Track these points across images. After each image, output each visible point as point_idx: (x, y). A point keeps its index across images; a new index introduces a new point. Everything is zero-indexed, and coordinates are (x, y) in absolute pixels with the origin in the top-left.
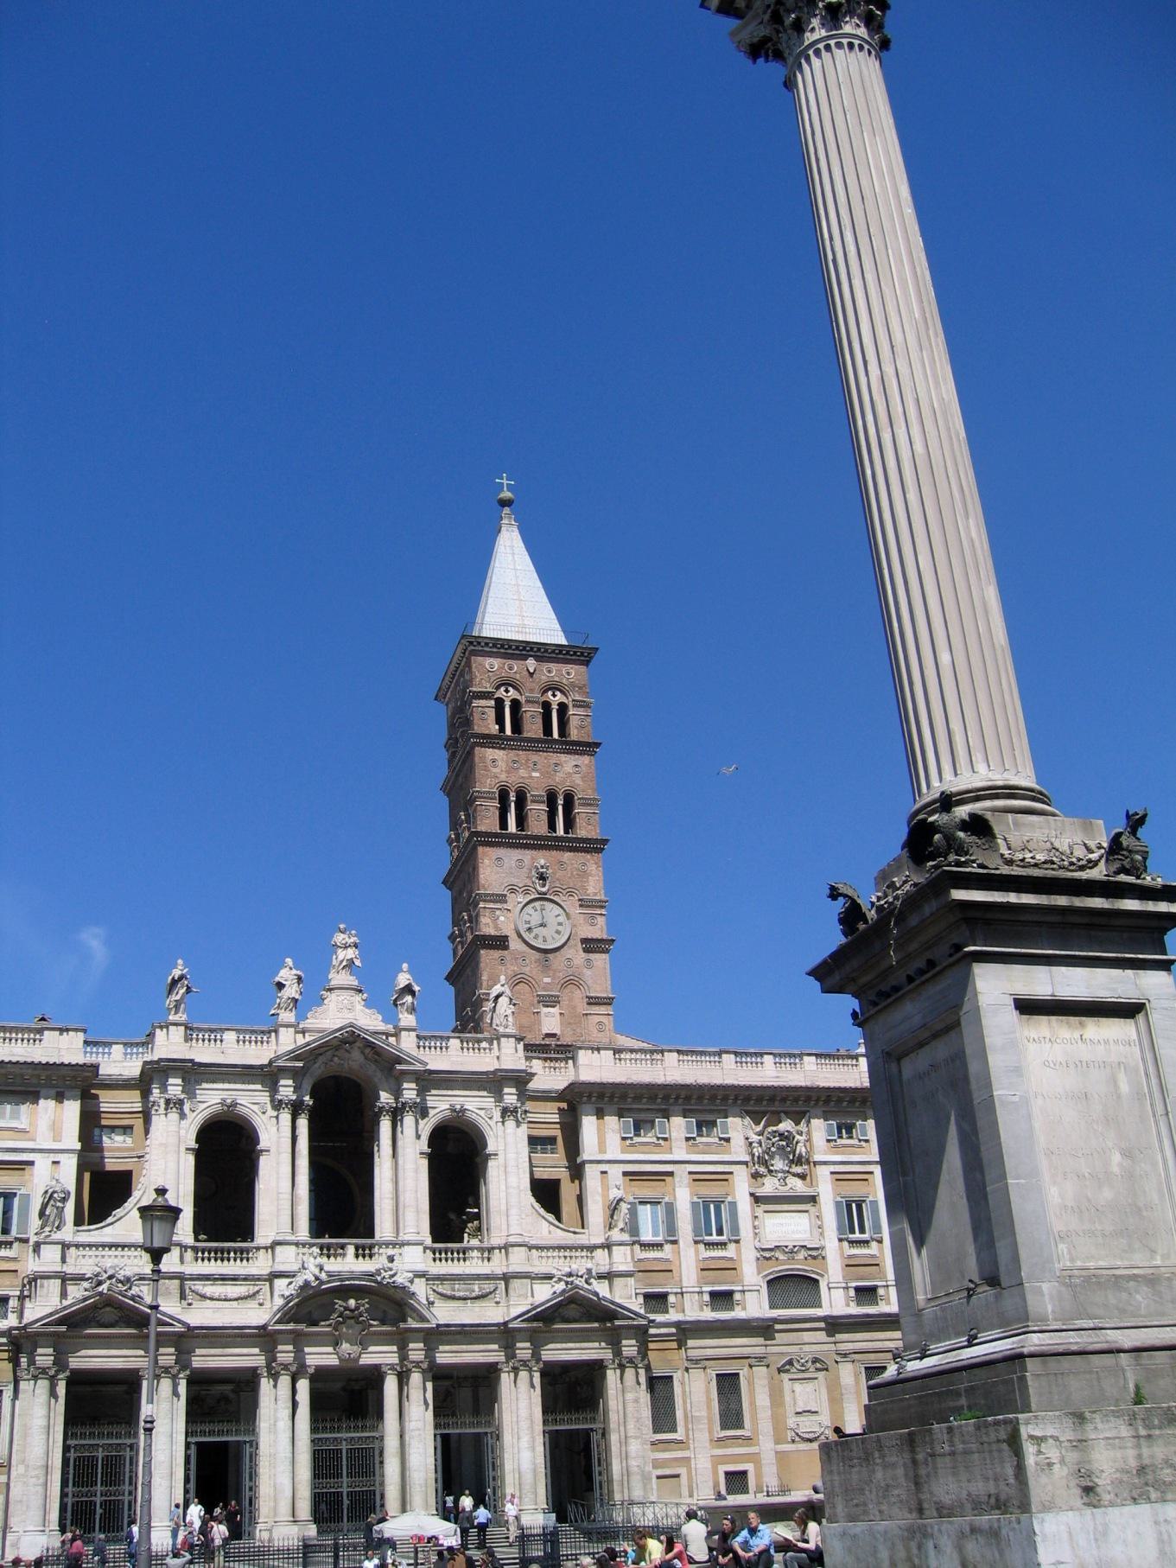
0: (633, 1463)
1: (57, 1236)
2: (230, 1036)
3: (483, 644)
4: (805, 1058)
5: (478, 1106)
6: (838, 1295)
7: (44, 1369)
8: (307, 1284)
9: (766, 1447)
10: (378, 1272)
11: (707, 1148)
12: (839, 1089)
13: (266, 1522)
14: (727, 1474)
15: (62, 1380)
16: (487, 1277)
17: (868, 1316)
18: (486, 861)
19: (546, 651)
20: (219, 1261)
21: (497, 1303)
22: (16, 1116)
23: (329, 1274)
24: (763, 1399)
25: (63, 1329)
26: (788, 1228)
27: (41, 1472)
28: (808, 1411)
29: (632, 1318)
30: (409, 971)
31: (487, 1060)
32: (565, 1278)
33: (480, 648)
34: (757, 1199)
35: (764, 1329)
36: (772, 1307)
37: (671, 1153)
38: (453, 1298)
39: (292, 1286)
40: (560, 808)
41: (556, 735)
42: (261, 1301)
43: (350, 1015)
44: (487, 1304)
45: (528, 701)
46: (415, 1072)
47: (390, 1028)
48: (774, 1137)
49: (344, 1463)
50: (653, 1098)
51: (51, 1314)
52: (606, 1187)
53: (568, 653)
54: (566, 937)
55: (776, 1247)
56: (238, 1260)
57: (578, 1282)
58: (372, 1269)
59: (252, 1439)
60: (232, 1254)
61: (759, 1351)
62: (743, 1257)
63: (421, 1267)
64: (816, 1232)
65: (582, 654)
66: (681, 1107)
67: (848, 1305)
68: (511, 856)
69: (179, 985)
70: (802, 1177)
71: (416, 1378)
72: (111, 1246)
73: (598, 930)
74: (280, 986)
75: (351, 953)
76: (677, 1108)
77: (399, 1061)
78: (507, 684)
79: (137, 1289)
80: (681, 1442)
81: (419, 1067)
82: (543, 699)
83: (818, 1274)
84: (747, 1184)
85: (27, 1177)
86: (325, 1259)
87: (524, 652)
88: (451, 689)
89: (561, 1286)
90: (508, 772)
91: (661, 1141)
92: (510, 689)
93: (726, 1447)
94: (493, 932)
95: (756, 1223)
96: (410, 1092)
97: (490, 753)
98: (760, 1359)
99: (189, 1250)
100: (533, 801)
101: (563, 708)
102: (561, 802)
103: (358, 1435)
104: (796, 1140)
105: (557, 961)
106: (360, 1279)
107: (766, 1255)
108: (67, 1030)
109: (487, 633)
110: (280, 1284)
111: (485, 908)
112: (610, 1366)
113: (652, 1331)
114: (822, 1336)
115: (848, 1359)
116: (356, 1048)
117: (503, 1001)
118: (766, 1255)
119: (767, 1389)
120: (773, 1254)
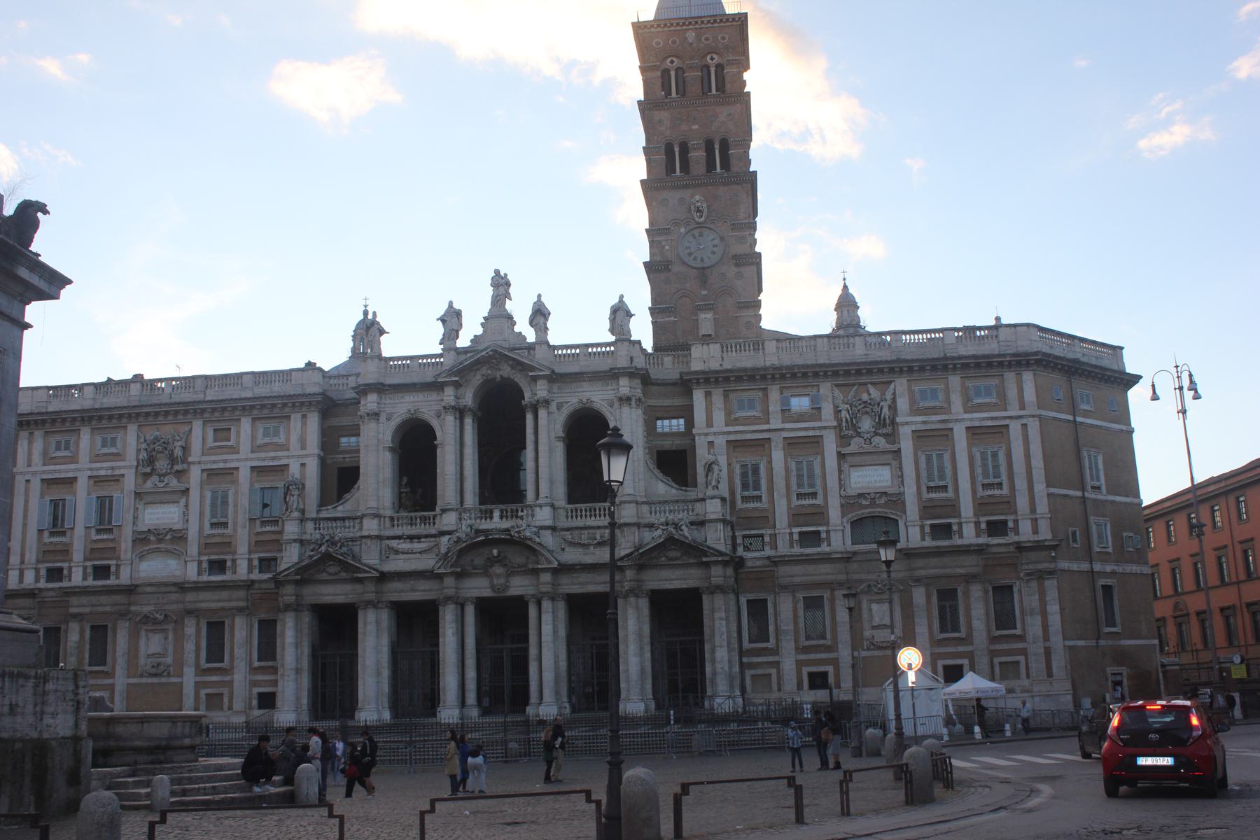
0: (718, 666)
5: (598, 396)
6: (915, 533)
7: (288, 605)
9: (845, 654)
10: (513, 527)
12: (917, 360)
14: (811, 675)
17: (938, 547)
19: (702, 22)
20: (409, 527)
22: (276, 433)
24: (843, 616)
27: (294, 672)
33: (648, 31)
34: (841, 456)
35: (848, 558)
36: (853, 544)
37: (769, 423)
38: (579, 544)
48: (860, 405)
50: (752, 378)
51: (289, 568)
53: (721, 20)
55: (861, 495)
61: (842, 577)
62: (829, 505)
63: (549, 523)
65: (734, 20)
66: (778, 386)
67: (923, 539)
68: (674, 196)
70: (886, 436)
71: (546, 605)
77: (532, 368)
80: (772, 649)
81: (547, 372)
83: (897, 515)
84: (834, 446)
86: (478, 521)
92: (674, 59)
93: (811, 653)
94: (658, 258)
98: (841, 584)
99: (387, 519)
100: (695, 149)
102: (717, 146)
107: (849, 503)
110: (445, 539)
113: (749, 564)
117: (620, 314)
118: (849, 503)
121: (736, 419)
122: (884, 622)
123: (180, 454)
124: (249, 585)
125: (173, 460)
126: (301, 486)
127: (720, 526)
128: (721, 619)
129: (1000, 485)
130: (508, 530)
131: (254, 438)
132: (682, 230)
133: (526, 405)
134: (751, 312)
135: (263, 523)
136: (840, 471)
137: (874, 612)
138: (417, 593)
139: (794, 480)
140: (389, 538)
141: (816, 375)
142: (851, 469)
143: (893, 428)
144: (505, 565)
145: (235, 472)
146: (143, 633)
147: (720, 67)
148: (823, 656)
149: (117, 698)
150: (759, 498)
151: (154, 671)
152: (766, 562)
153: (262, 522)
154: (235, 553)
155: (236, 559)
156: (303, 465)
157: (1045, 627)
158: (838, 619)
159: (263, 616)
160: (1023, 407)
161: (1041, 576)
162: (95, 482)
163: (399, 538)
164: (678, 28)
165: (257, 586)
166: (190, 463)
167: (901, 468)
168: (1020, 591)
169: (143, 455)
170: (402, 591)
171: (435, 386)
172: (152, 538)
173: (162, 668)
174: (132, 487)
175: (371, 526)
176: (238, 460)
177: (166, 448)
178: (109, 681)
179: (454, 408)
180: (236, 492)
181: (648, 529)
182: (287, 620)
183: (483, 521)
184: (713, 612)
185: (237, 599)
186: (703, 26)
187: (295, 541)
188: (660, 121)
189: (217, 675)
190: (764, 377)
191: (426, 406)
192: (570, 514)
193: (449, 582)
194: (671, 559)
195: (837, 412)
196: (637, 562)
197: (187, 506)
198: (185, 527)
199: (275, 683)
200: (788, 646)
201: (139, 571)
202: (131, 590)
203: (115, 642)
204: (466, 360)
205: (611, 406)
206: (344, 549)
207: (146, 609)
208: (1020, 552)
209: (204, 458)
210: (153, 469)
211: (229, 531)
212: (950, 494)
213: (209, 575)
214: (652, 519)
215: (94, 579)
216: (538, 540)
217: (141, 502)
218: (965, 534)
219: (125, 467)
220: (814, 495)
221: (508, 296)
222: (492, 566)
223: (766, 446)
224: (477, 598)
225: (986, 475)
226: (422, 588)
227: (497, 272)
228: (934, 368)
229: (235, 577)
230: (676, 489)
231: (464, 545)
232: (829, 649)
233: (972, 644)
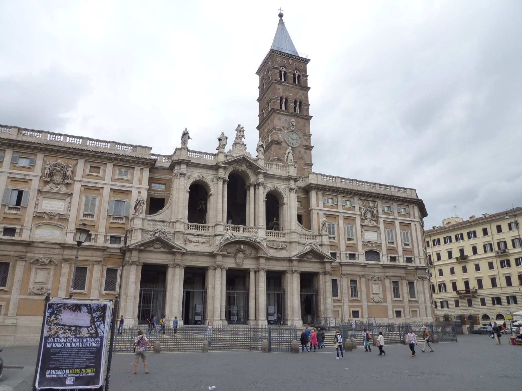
1: (141, 216)
4: (377, 185)
5: (281, 186)
6: (385, 258)
7: (134, 262)
8: (228, 239)
9: (365, 304)
11: (348, 209)
14: (353, 312)
15: (140, 266)
16: (284, 242)
17: (394, 265)
18: (276, 118)
19: (295, 58)
20: (196, 230)
21: (287, 251)
22: (126, 174)
23: (234, 236)
24: (364, 288)
25: (142, 248)
26: (371, 236)
27: (133, 298)
28: (377, 293)
34: (362, 226)
37: (338, 209)
38: (273, 248)
41: (297, 83)
43: (242, 153)
44: (284, 251)
51: (138, 242)
52: (319, 218)
55: (368, 242)
56: (203, 230)
57: (313, 246)
60: (201, 227)
61: (363, 273)
62: (359, 244)
63: (265, 236)
64: (379, 238)
65: (306, 61)
68: (284, 118)
69: (186, 135)
70: (375, 221)
72: (159, 221)
76: (340, 196)
77: (259, 168)
79: (169, 236)
80: (339, 300)
81: (265, 171)
82: (293, 73)
83: (379, 251)
84: (360, 221)
85: (129, 196)
86: (233, 231)
87: (289, 58)
89: (308, 247)
90: (283, 92)
91: (335, 205)
92: (284, 68)
94: (277, 139)
97: (278, 86)
98: (363, 276)
100: (291, 102)
101: (299, 76)
106: (244, 238)
107: (366, 244)
110: (218, 238)
114: (381, 270)
116: (244, 164)
117: (290, 155)
121: (326, 206)
123: (71, 174)
124: (104, 249)
125: (65, 176)
127: (329, 247)
128: (329, 286)
129: (408, 245)
130: (249, 238)
131: (113, 174)
132: (286, 131)
133: (251, 184)
134: (309, 168)
135: (114, 218)
136: (362, 232)
137: (373, 288)
138: (199, 263)
139: (346, 233)
140: (187, 234)
141: (354, 194)
142: (365, 231)
143: (377, 219)
144: (244, 254)
145: (101, 190)
146: (34, 270)
147: (299, 76)
148: (357, 304)
149: (11, 306)
150: (334, 238)
151: (38, 292)
152: (338, 264)
153: (113, 217)
154: (97, 231)
155: (97, 235)
156: (140, 192)
157: (425, 298)
158: (362, 290)
159: (111, 267)
160: (415, 218)
161: (423, 279)
162: (12, 180)
163: (192, 235)
165: (108, 250)
166: (75, 181)
168: (416, 284)
169: (47, 171)
170: (191, 261)
171: (216, 168)
172: (46, 217)
173: (44, 291)
174: (37, 188)
175: (180, 227)
176: (104, 184)
177: (62, 170)
178: (7, 296)
179: (223, 178)
180: (101, 201)
181: (300, 245)
182: (132, 270)
183: (235, 231)
184: (325, 282)
185: (98, 256)
186: (295, 59)
187: (140, 229)
188: (279, 89)
190: (337, 192)
191: (208, 176)
192: (268, 234)
193: (219, 258)
194: (308, 259)
195: (360, 209)
196: (300, 258)
198: (68, 213)
200: (346, 299)
201: (35, 234)
202: (29, 244)
203: (13, 273)
204: (232, 159)
206: (168, 237)
207: (37, 256)
208: (416, 270)
209: (84, 179)
210: (50, 180)
212: (395, 246)
214: (302, 241)
215: (3, 235)
216: (262, 244)
217: (41, 196)
219: (33, 176)
220: (352, 240)
221: (243, 136)
222: (239, 253)
223: (337, 218)
224: (229, 268)
226: (202, 260)
227: (239, 126)
228: (390, 199)
229: (95, 244)
230: (305, 230)
231: (229, 241)
232: (359, 301)
233: (404, 303)
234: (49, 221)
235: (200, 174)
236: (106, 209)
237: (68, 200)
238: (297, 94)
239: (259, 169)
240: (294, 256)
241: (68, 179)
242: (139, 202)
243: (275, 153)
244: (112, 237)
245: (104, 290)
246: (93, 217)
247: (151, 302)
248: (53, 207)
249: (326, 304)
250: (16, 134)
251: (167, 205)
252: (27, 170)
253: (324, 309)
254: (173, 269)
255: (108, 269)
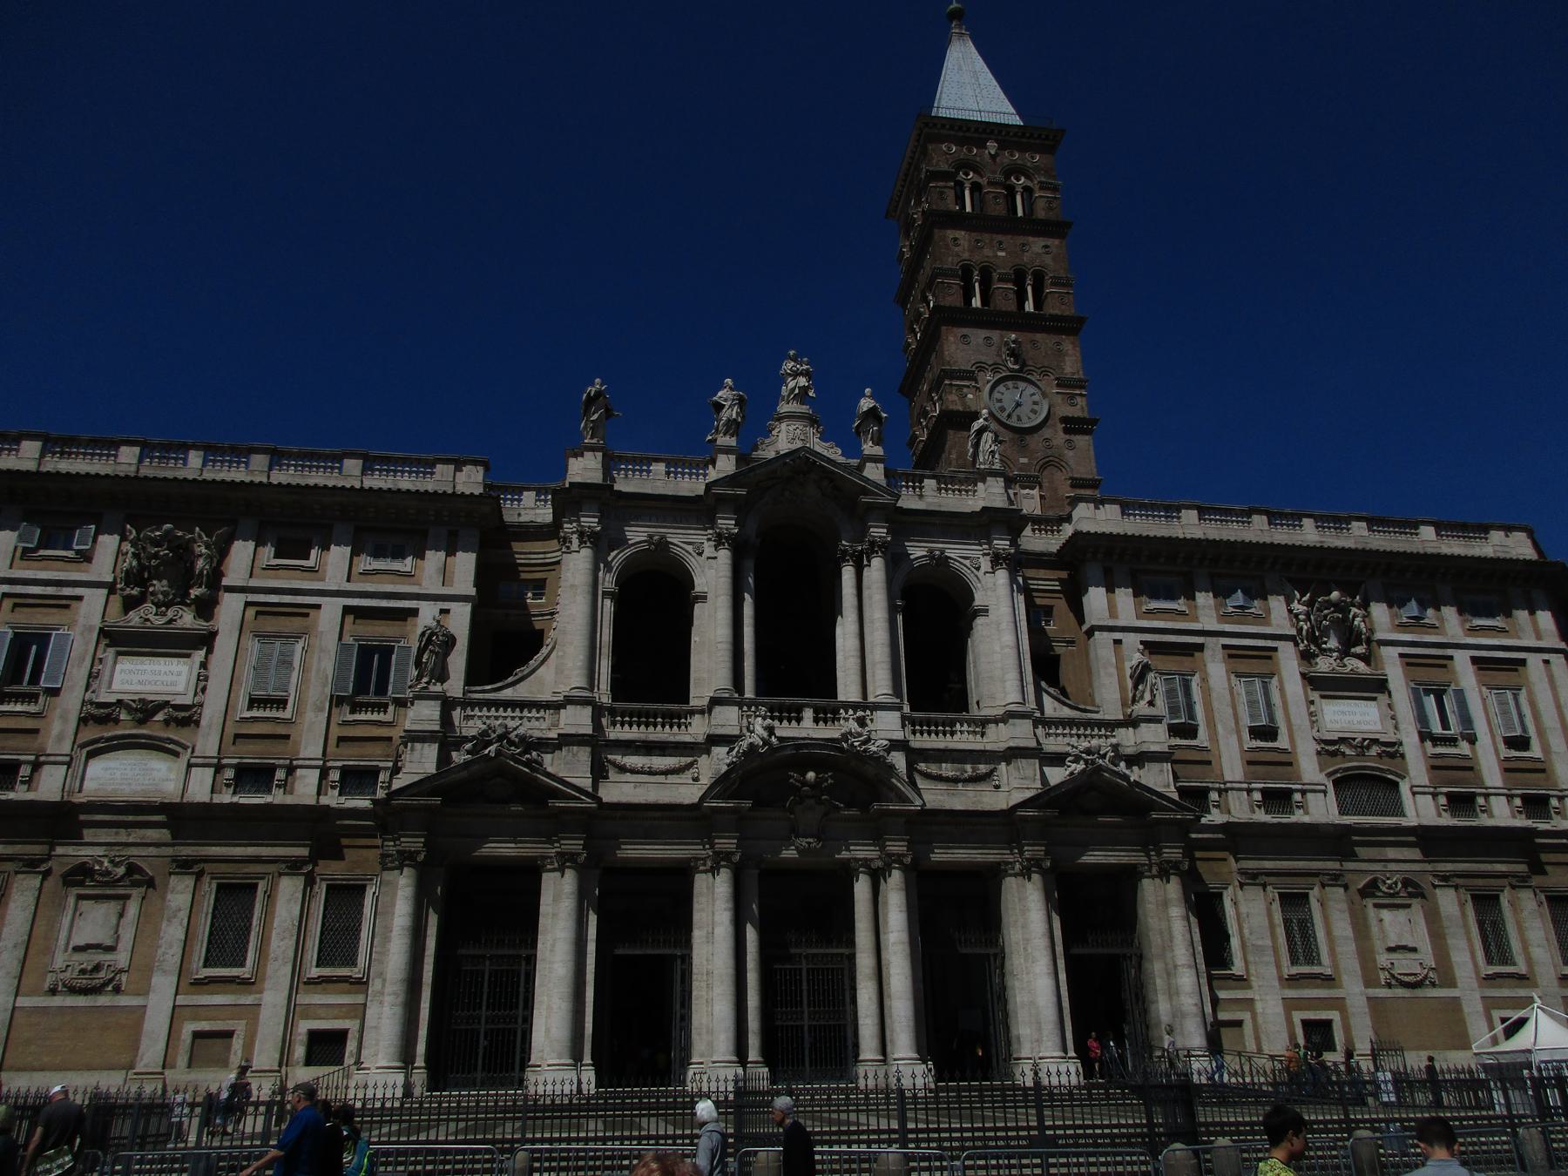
2: (660, 468)
3: (939, 126)
9: (1353, 990)
10: (845, 737)
13: (702, 1063)
21: (997, 787)
23: (780, 739)
24: (1343, 927)
25: (437, 800)
29: (1173, 810)
30: (872, 396)
31: (970, 502)
32: (1084, 755)
36: (1341, 813)
37: (1196, 619)
39: (734, 753)
40: (1029, 289)
42: (696, 775)
45: (990, 183)
46: (883, 507)
47: (854, 462)
49: (805, 987)
52: (1120, 659)
54: (1044, 415)
55: (1342, 740)
58: (836, 735)
59: (685, 952)
63: (899, 735)
67: (1439, 815)
68: (978, 335)
73: (1079, 409)
74: (719, 407)
75: (803, 381)
77: (866, 492)
78: (966, 165)
84: (1296, 662)
85: (409, 628)
86: (776, 723)
88: (903, 197)
89: (1081, 766)
93: (1303, 987)
94: (961, 409)
95: (1312, 708)
96: (879, 532)
97: (951, 234)
100: (1000, 280)
103: (822, 951)
104: (1352, 613)
105: (1035, 441)
107: (1329, 749)
108: (465, 463)
109: (943, 113)
110: (720, 752)
111: (951, 384)
112: (1146, 874)
115: (1450, 883)
117: (988, 437)
118: (1329, 749)
119: (1346, 916)
120: (1337, 747)
122: (1403, 943)
126: (450, 642)
142: (1323, 700)
143: (1369, 648)
145: (312, 612)
160: (1539, 637)
164: (976, 135)
167: (1390, 706)
169: (129, 562)
174: (96, 622)
175: (577, 720)
188: (955, 239)
189: (225, 993)
197: (204, 665)
199: (360, 1012)
205: (978, 569)
210: (141, 592)
211: (287, 714)
213: (235, 793)
214: (1053, 744)
218: (1496, 811)
225: (1509, 725)
229: (289, 800)
232: (1328, 981)
234: (134, 731)
235: (654, 530)
236: (327, 678)
237: (199, 655)
238: (1023, 251)
239: (866, 494)
240: (1024, 804)
241: (200, 587)
242: (429, 641)
243: (954, 456)
244: (346, 772)
245: (314, 963)
246: (284, 708)
247: (481, 1003)
248: (150, 683)
249: (1178, 994)
250: (37, 456)
251: (544, 651)
252: (69, 566)
253: (1174, 1016)
254: (558, 874)
255: (329, 887)
